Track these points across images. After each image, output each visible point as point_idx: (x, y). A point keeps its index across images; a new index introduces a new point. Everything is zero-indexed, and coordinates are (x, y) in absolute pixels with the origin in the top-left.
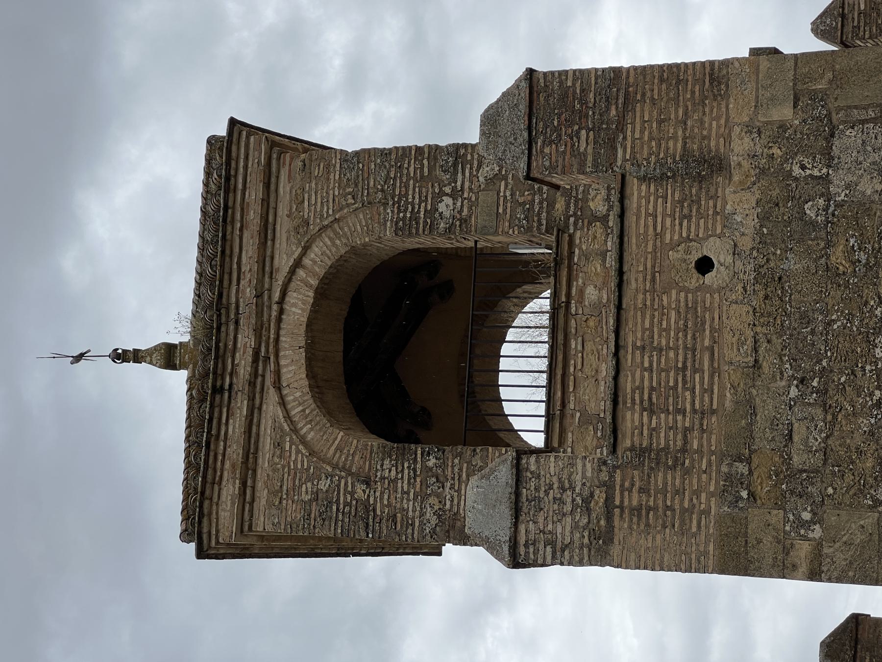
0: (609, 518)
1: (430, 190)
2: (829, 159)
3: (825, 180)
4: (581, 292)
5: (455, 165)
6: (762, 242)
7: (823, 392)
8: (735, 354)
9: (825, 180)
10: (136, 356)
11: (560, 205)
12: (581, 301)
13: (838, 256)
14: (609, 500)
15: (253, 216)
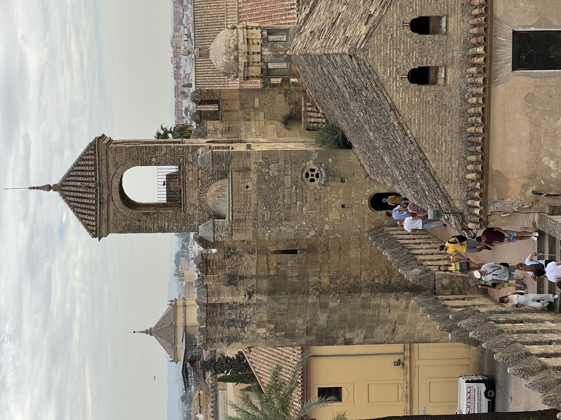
0: (232, 232)
1: (150, 156)
2: (269, 169)
3: (269, 172)
4: (188, 178)
5: (155, 150)
6: (258, 183)
7: (269, 208)
8: (254, 202)
9: (269, 172)
10: (38, 188)
11: (181, 160)
12: (188, 180)
13: (271, 185)
14: (232, 229)
15: (104, 162)
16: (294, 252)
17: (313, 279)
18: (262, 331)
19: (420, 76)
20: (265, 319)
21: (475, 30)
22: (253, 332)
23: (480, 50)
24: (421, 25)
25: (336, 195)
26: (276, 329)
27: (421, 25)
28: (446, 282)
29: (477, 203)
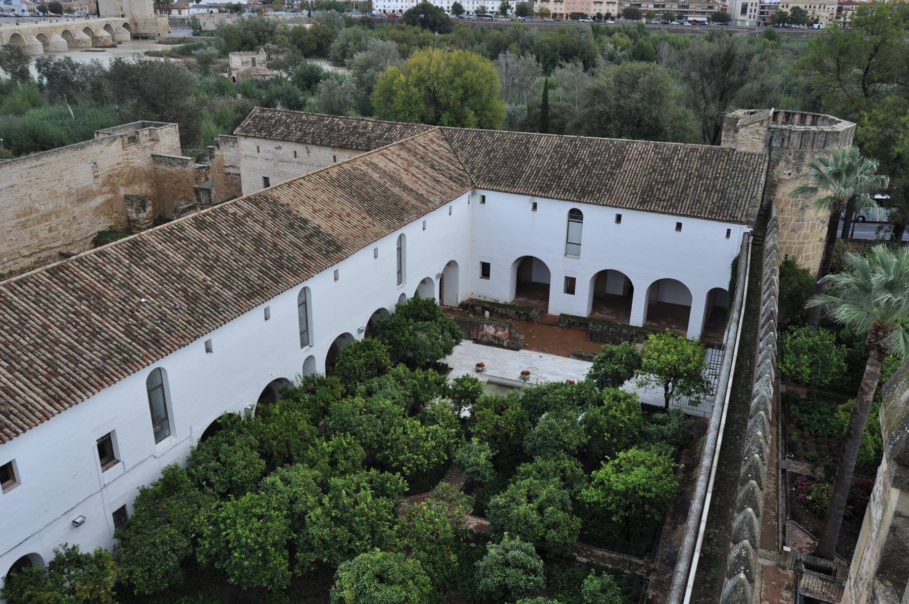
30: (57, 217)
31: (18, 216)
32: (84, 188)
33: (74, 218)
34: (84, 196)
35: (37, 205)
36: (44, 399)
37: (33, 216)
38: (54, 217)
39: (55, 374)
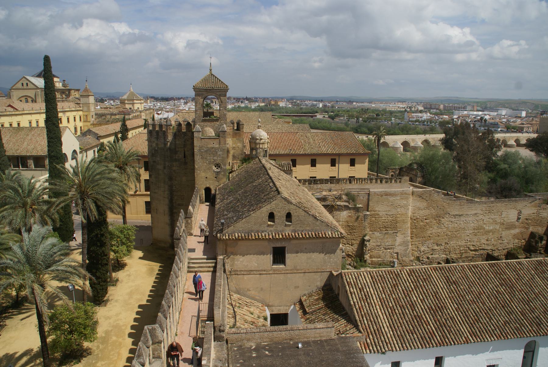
16: (185, 157)
17: (174, 164)
18: (154, 145)
19: (271, 216)
20: (159, 146)
21: (287, 234)
22: (154, 142)
23: (281, 236)
24: (289, 216)
25: (210, 175)
26: (155, 150)
27: (289, 216)
28: (189, 221)
29: (227, 237)
30: (493, 234)
31: (474, 229)
32: (511, 222)
33: (501, 237)
34: (510, 227)
35: (485, 226)
36: (469, 332)
37: (482, 231)
38: (491, 234)
39: (478, 321)
